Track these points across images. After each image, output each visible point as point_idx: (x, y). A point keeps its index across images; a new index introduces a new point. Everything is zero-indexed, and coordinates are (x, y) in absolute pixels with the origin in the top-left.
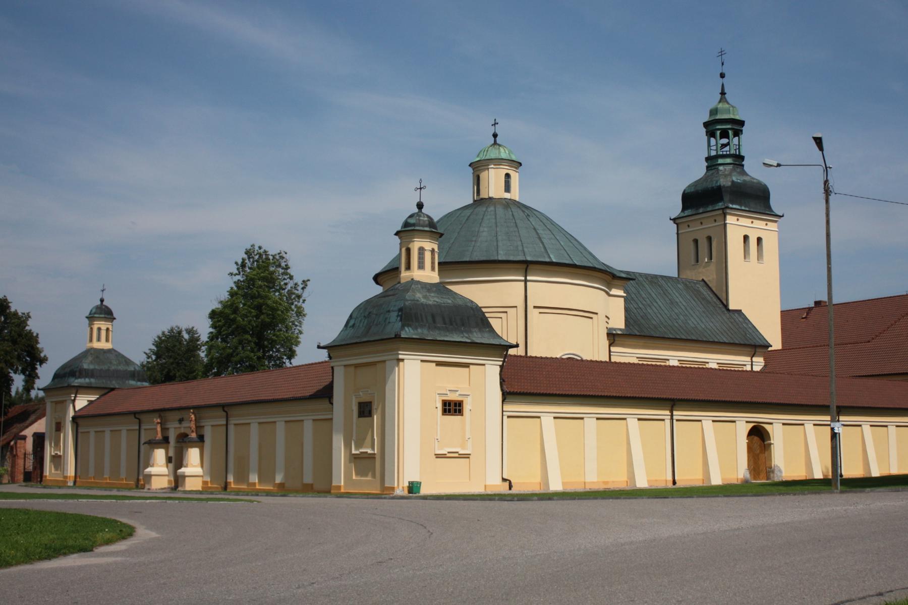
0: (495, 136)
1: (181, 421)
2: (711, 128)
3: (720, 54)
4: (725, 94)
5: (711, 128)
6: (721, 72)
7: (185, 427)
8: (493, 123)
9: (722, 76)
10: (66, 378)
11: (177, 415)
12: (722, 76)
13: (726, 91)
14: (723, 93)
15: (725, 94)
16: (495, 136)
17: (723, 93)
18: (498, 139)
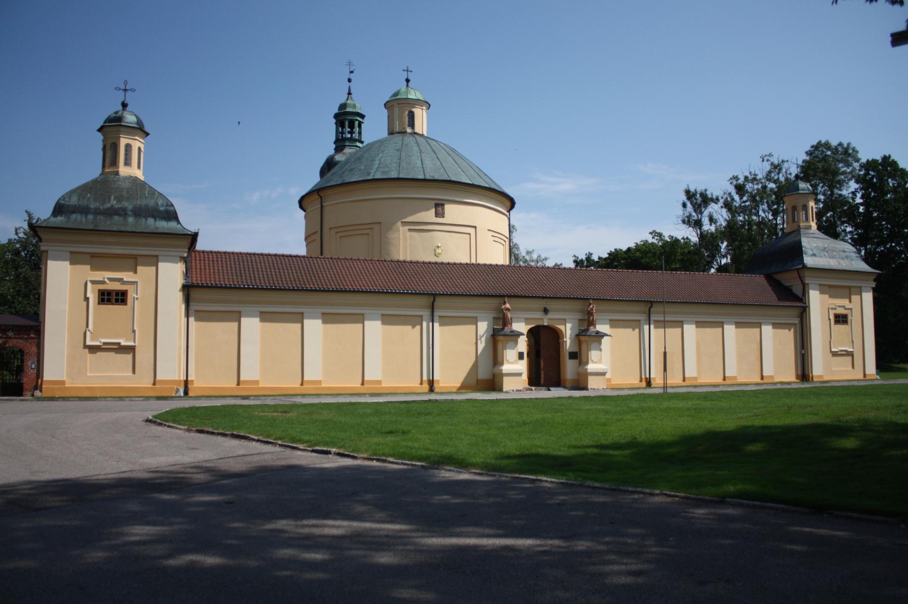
0: (408, 81)
1: (546, 311)
2: (342, 118)
3: (348, 64)
4: (351, 94)
5: (342, 118)
6: (348, 77)
7: (549, 319)
8: (406, 69)
9: (350, 80)
10: (131, 220)
11: (542, 304)
12: (350, 80)
13: (351, 92)
14: (349, 94)
15: (351, 94)
16: (408, 81)
17: (349, 94)
18: (410, 84)
